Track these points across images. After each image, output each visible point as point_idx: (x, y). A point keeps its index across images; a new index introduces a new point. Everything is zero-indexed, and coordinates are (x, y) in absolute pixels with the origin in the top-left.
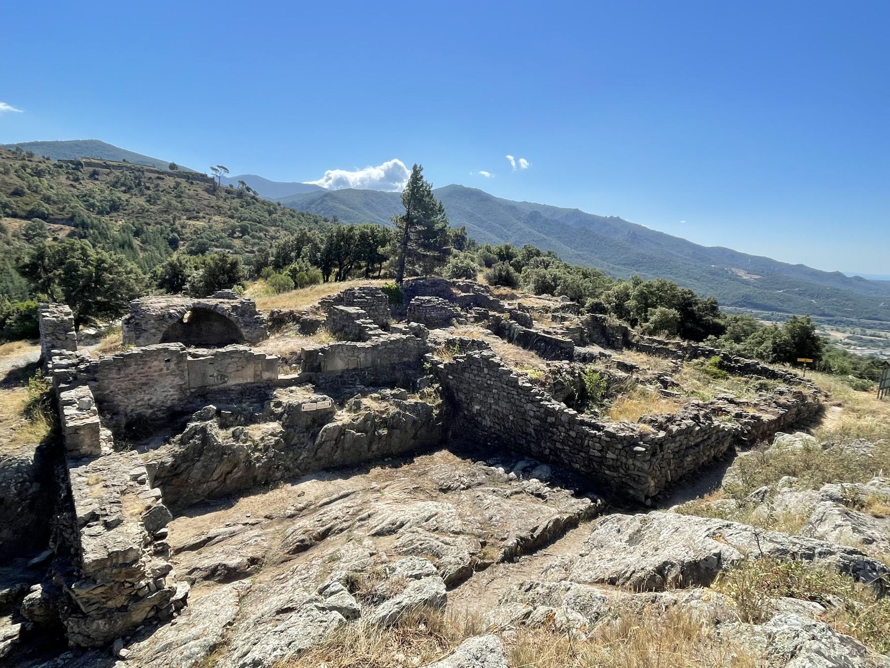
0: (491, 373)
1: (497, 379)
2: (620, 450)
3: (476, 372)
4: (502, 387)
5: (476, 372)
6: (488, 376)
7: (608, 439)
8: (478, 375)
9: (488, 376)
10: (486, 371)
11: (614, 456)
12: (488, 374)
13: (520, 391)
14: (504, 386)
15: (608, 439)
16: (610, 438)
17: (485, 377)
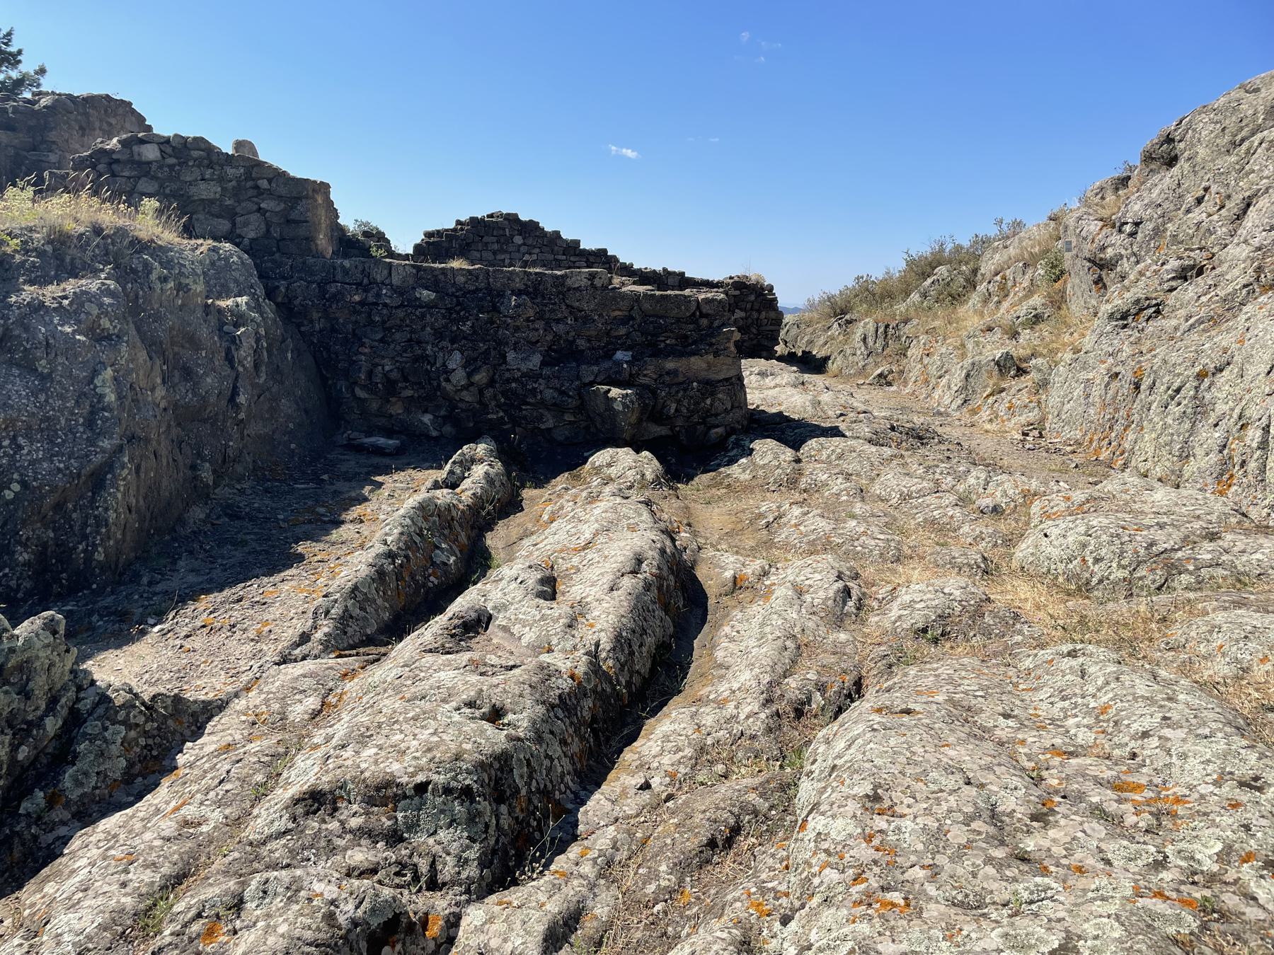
0: (530, 241)
1: (545, 249)
2: (753, 302)
3: (496, 247)
4: (556, 260)
5: (496, 247)
6: (523, 249)
7: (737, 293)
8: (502, 251)
9: (523, 249)
10: (518, 240)
11: (743, 314)
12: (524, 244)
13: (592, 259)
14: (560, 257)
15: (737, 293)
16: (740, 290)
17: (519, 251)
